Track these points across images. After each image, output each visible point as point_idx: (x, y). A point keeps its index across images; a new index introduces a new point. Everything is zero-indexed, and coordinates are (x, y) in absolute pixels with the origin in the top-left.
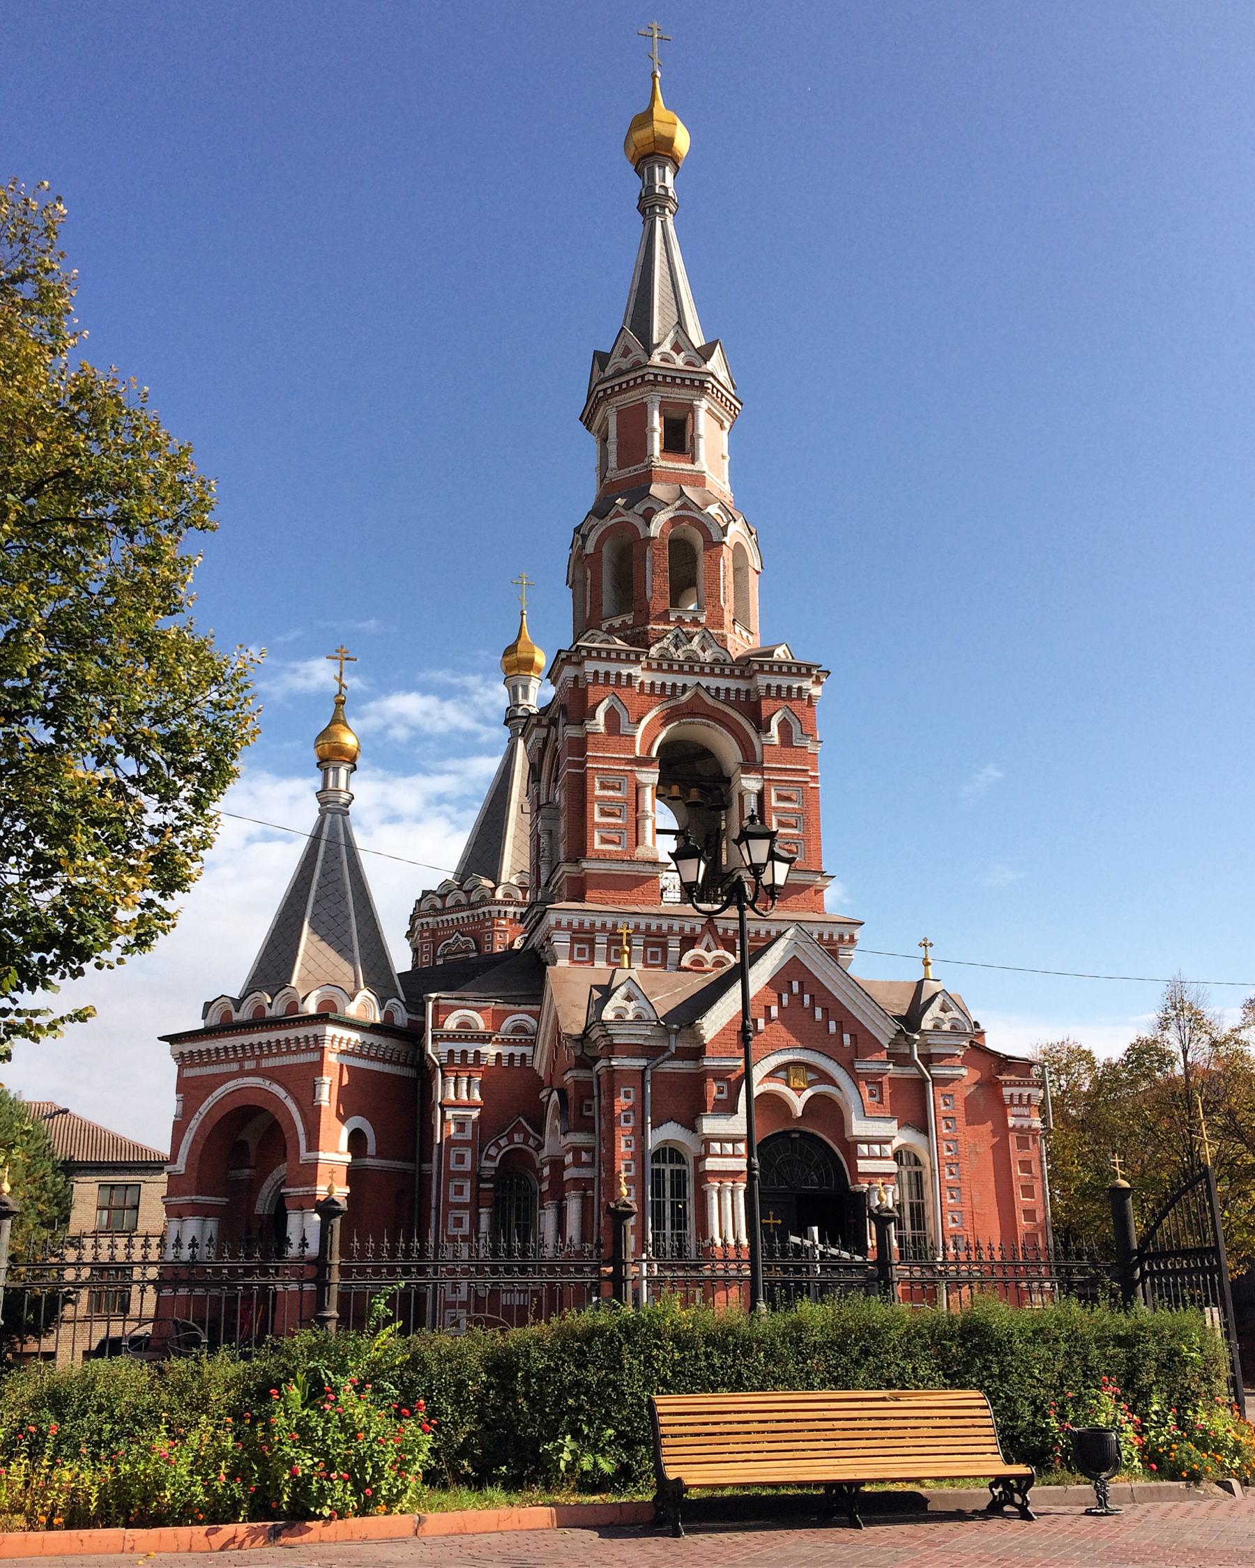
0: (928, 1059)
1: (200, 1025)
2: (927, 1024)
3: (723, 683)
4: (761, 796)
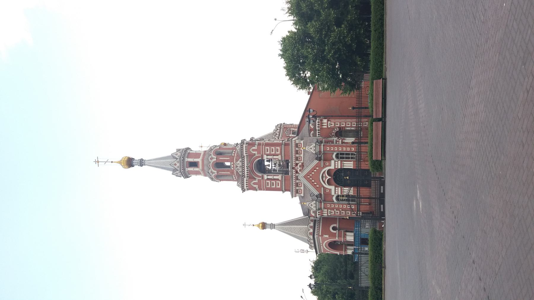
0: (320, 151)
1: (314, 250)
3: (246, 161)
4: (267, 155)
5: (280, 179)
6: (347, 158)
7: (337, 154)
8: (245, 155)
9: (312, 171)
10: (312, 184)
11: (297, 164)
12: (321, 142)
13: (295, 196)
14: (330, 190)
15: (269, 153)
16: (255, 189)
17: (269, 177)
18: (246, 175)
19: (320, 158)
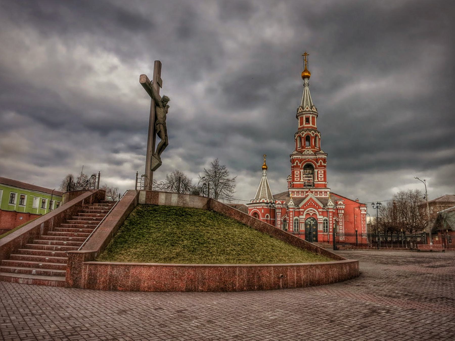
0: (329, 209)
1: (249, 203)
2: (328, 204)
4: (318, 172)
6: (324, 226)
7: (326, 220)
8: (317, 156)
9: (316, 203)
10: (307, 203)
11: (312, 192)
12: (334, 209)
14: (303, 215)
17: (302, 173)
18: (302, 157)
19: (325, 209)
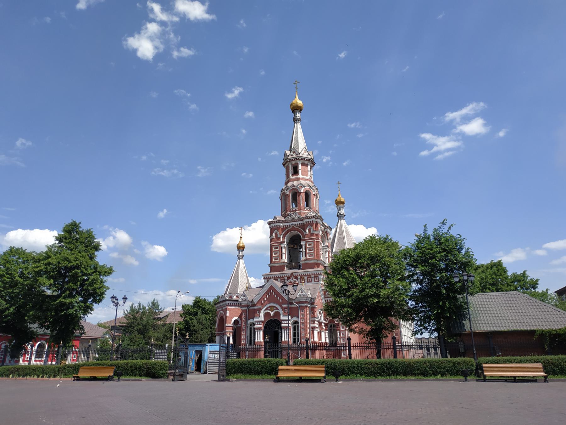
4: (305, 245)
5: (282, 261)
13: (264, 278)
15: (308, 246)
16: (271, 235)
